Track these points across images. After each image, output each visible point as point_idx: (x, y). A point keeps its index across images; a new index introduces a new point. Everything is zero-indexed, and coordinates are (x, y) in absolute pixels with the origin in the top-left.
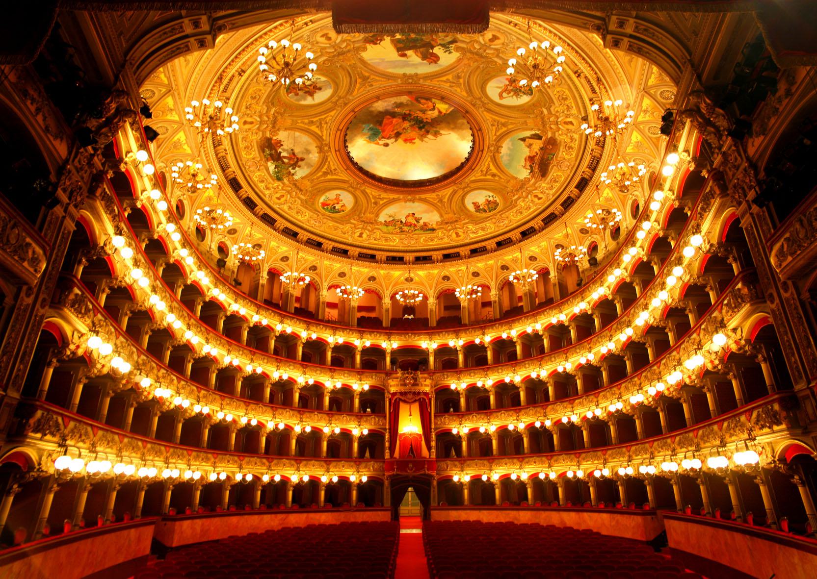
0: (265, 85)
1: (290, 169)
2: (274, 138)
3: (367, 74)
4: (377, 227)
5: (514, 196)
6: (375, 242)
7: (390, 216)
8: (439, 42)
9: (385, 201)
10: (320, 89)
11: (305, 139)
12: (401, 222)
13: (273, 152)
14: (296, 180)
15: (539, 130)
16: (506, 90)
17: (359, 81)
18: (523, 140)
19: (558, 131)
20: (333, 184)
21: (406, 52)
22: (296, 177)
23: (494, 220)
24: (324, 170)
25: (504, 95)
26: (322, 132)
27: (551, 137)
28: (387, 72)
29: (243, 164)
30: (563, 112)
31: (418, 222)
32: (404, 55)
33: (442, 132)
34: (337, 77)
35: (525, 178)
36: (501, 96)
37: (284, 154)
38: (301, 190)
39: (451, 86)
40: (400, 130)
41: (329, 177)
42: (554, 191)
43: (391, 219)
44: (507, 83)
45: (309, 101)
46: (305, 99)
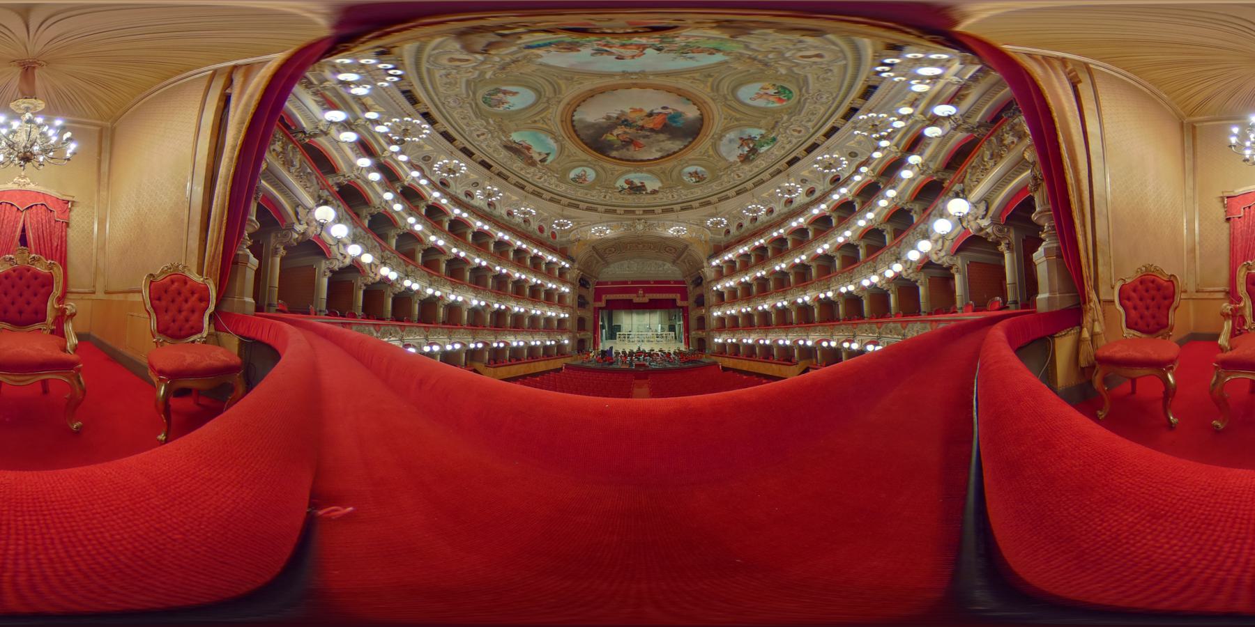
10: (690, 173)
13: (750, 154)
16: (584, 175)
17: (667, 172)
18: (548, 154)
25: (583, 173)
32: (642, 183)
45: (700, 169)
46: (701, 171)
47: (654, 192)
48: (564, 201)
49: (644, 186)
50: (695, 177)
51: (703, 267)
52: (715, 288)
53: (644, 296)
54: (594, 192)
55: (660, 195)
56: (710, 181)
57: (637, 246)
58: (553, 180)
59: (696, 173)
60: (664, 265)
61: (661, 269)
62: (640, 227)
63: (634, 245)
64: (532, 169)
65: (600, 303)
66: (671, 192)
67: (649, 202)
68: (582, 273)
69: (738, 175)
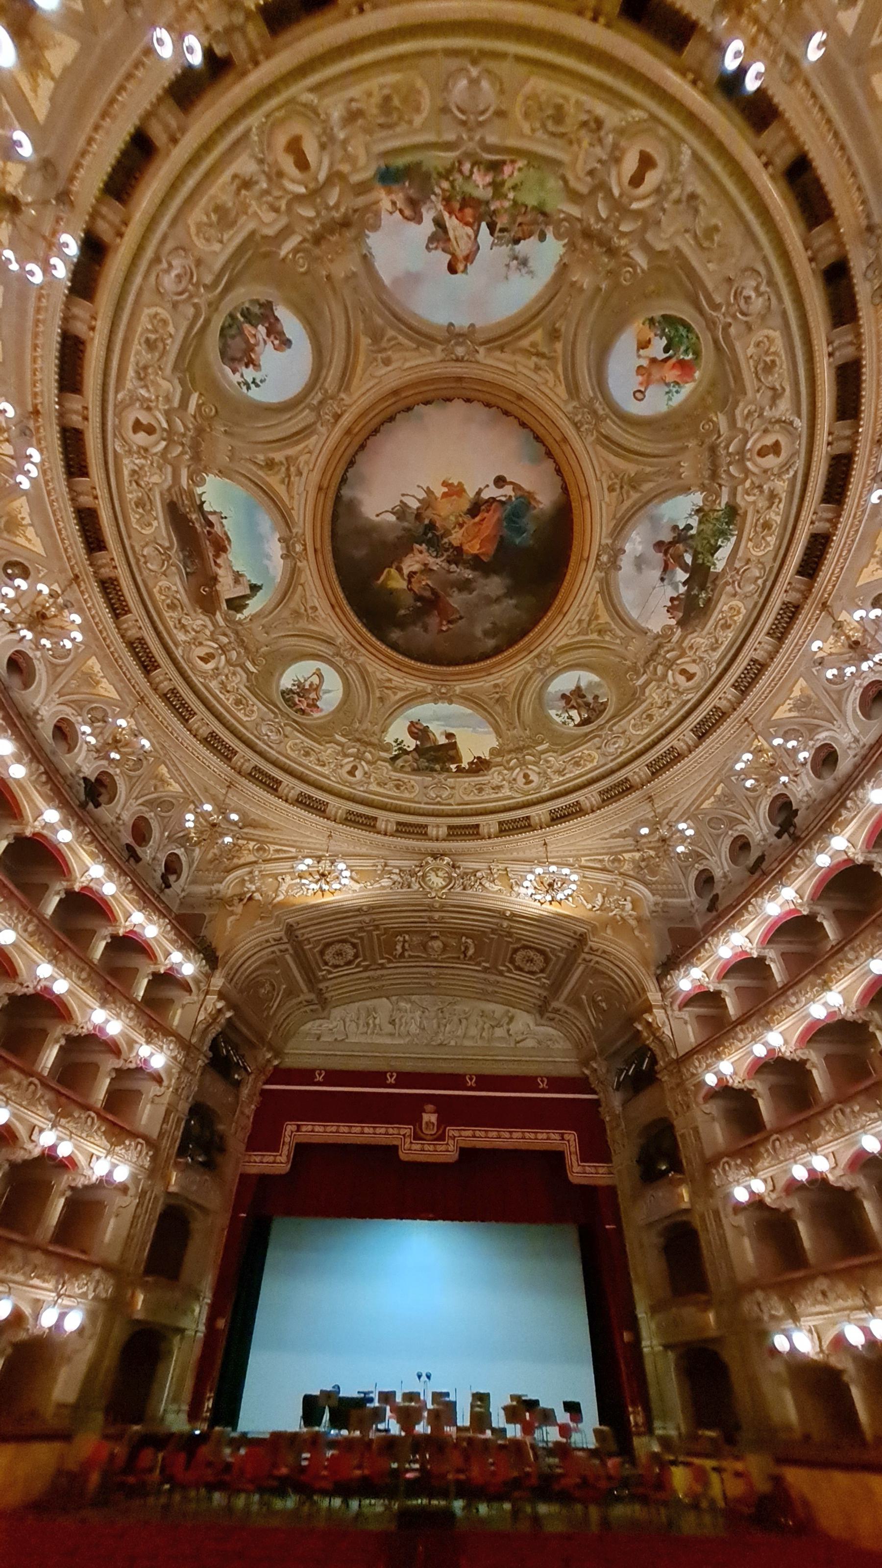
0: (624, 733)
1: (693, 532)
2: (673, 622)
3: (498, 708)
4: (575, 211)
5: (199, 406)
6: (601, 109)
7: (524, 262)
8: (409, 757)
9: (525, 343)
10: (564, 696)
11: (628, 597)
12: (492, 227)
13: (695, 592)
14: (703, 488)
15: (240, 623)
16: (316, 689)
18: (255, 588)
19: (212, 633)
20: (632, 442)
21: (447, 741)
22: (697, 498)
23: (208, 279)
24: (635, 496)
25: (316, 680)
26: (595, 604)
27: (214, 614)
28: (471, 708)
29: (760, 596)
30: (227, 676)
31: (439, 223)
32: (449, 736)
33: (392, 518)
34: (534, 710)
35: (203, 482)
36: (321, 676)
37: (682, 576)
38: (713, 449)
39: (390, 680)
40: (470, 522)
41: (631, 469)
42: (126, 473)
43: (523, 247)
44: (318, 703)
45: (586, 678)
46: (590, 684)
47: (480, 766)
48: (246, 758)
49: (453, 746)
50: (577, 707)
51: (649, 1009)
52: (711, 1080)
53: (441, 1138)
54: (328, 751)
55: (493, 777)
56: (620, 715)
57: (424, 947)
58: (238, 681)
59: (578, 692)
60: (511, 1019)
61: (499, 1032)
62: (437, 881)
63: (416, 939)
64: (198, 621)
65: (269, 1157)
66: (522, 763)
67: (467, 798)
68: (229, 1014)
69: (683, 672)
